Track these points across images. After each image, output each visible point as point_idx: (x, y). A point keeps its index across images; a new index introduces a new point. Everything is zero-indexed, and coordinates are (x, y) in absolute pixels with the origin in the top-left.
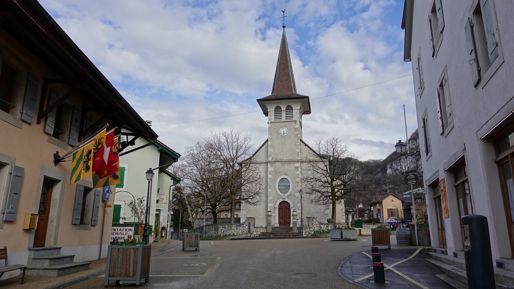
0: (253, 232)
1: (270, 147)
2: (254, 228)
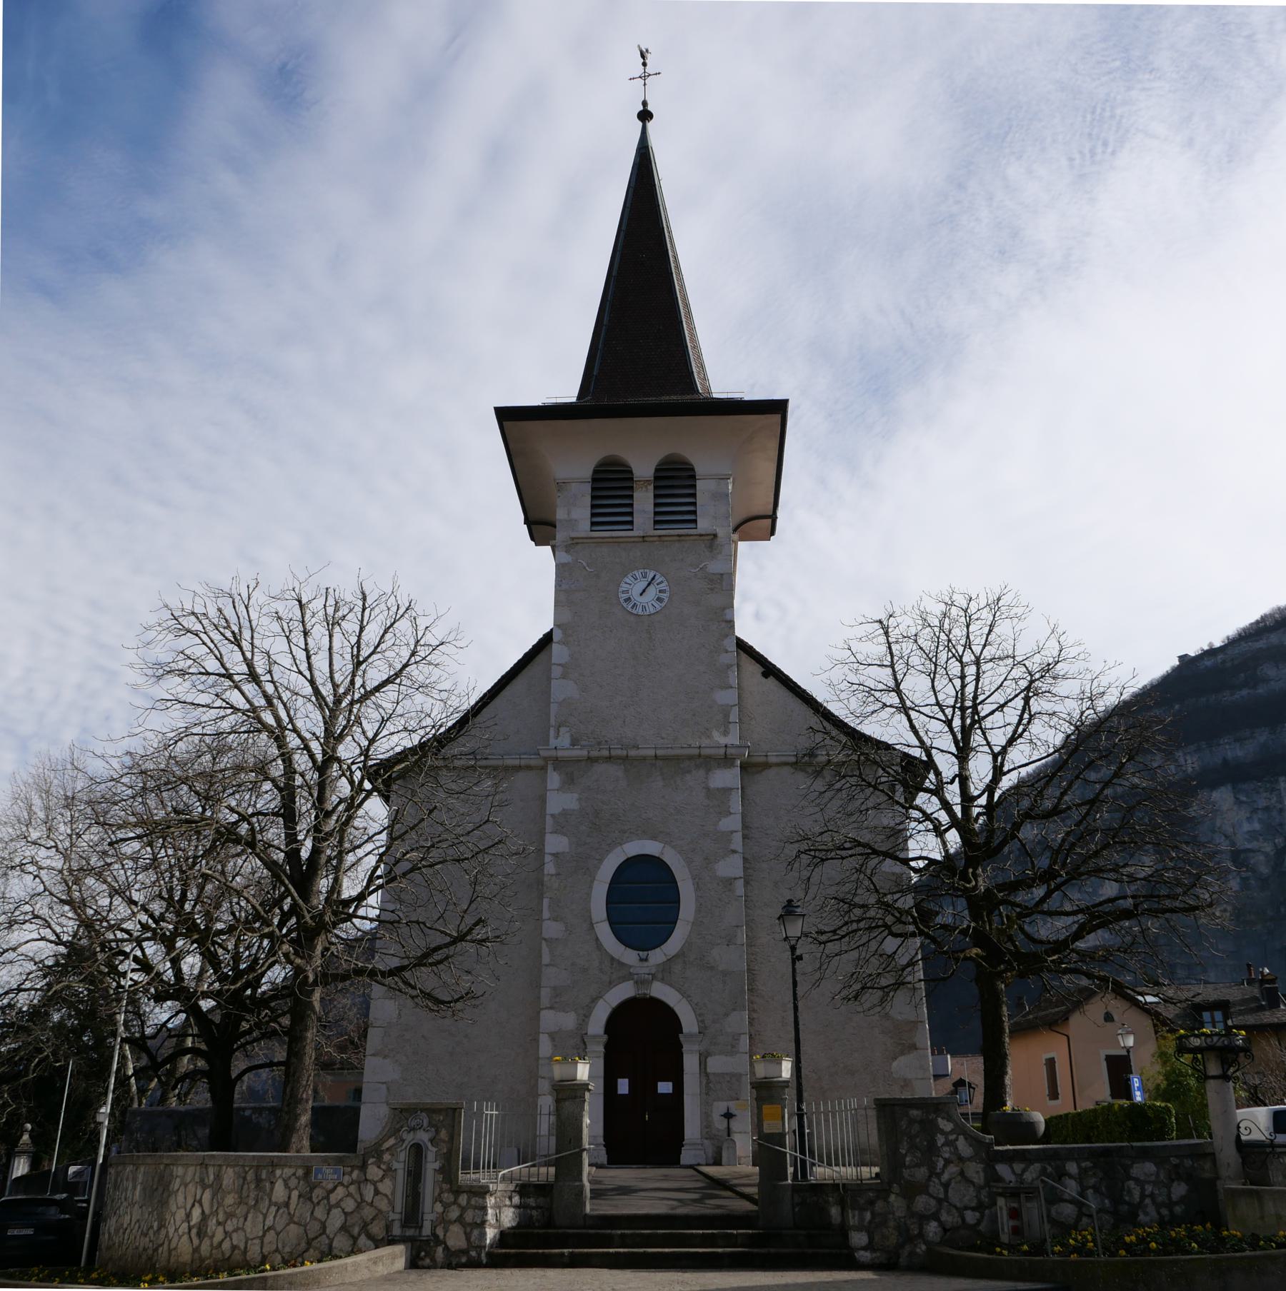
0: (440, 1232)
1: (564, 676)
2: (448, 1197)
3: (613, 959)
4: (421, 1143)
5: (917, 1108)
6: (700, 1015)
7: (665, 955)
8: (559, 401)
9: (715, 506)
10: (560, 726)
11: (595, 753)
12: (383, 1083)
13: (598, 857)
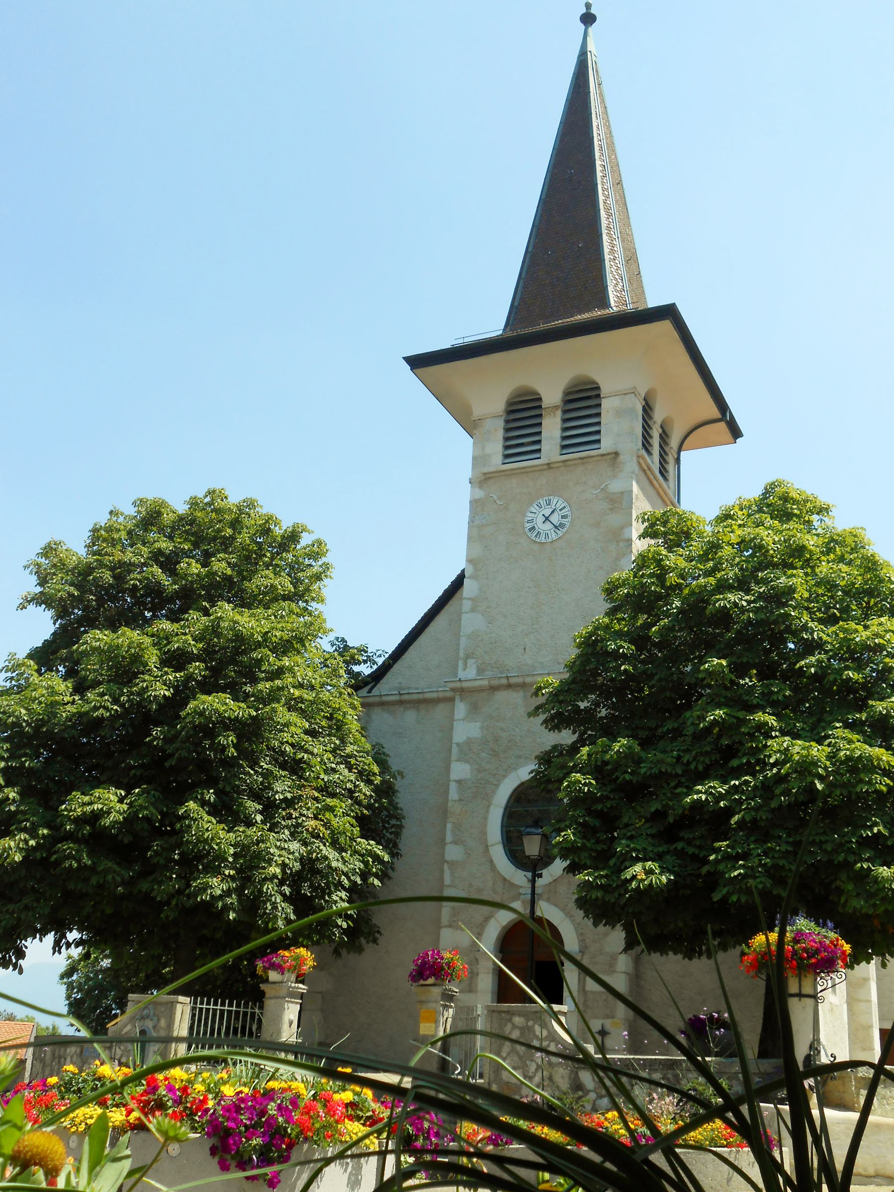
1: (473, 610)
3: (505, 880)
4: (147, 1030)
5: (519, 1015)
6: (582, 934)
7: (551, 875)
8: (466, 340)
9: (619, 422)
10: (467, 658)
11: (495, 682)
12: (319, 993)
13: (495, 783)
